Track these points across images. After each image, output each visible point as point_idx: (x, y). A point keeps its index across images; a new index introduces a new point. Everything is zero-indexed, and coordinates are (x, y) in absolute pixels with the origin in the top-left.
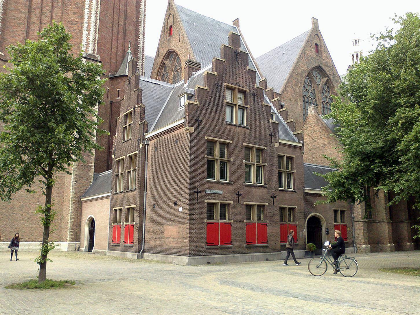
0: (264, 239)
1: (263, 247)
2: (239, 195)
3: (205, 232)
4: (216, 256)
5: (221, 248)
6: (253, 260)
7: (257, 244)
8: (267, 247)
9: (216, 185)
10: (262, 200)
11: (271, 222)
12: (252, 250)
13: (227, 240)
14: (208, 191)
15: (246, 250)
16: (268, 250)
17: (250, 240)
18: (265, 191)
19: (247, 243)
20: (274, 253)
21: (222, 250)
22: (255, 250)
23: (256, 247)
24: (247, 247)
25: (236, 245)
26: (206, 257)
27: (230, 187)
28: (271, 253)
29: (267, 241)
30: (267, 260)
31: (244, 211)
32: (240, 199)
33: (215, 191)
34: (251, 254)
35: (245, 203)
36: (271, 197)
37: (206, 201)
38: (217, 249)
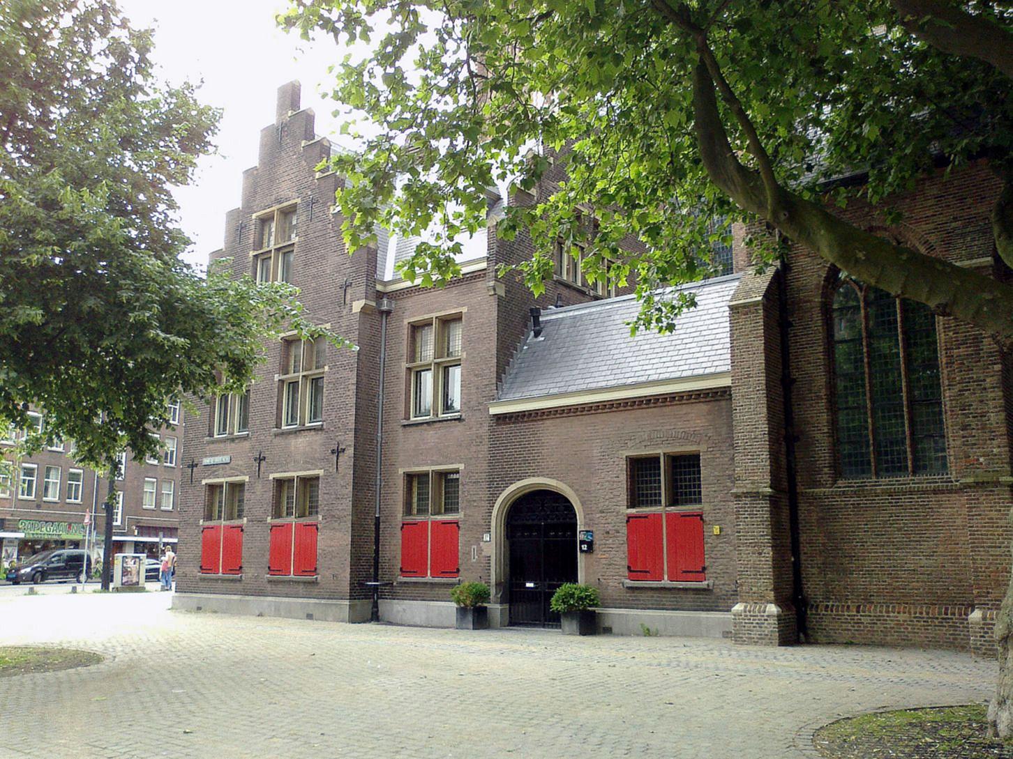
0: (308, 562)
1: (305, 583)
2: (261, 459)
3: (200, 547)
4: (212, 596)
5: (223, 580)
6: (278, 612)
7: (292, 576)
8: (315, 583)
9: (222, 445)
10: (310, 462)
11: (328, 520)
12: (280, 588)
13: (235, 566)
14: (206, 461)
15: (269, 587)
16: (315, 590)
17: (277, 565)
18: (318, 438)
19: (273, 573)
20: (330, 602)
21: (227, 585)
22: (284, 589)
23: (289, 582)
24: (270, 582)
25: (250, 575)
26: (194, 595)
27: (247, 445)
28: (323, 601)
29: (316, 569)
30: (310, 617)
31: (270, 495)
32: (262, 469)
33: (218, 460)
34: (278, 599)
35: (271, 476)
36: (333, 452)
37: (204, 482)
38: (217, 580)
